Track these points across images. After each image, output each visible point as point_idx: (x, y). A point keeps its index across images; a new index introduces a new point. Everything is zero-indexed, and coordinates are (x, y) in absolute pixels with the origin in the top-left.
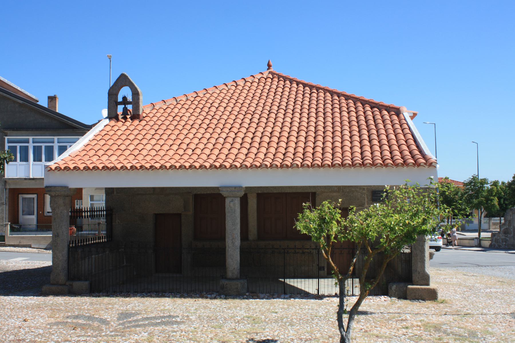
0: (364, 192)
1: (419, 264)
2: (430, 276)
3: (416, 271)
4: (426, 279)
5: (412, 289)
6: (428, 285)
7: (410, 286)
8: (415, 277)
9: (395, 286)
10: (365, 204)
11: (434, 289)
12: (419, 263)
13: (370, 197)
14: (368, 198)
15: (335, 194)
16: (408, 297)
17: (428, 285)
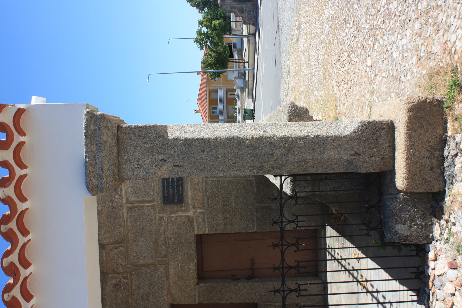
0: (166, 219)
1: (330, 154)
2: (365, 118)
3: (350, 162)
4: (378, 133)
5: (411, 174)
6: (390, 127)
7: (400, 182)
8: (369, 165)
9: (399, 227)
10: (188, 217)
11: (410, 110)
12: (327, 154)
13: (176, 207)
14: (178, 211)
15: (172, 271)
16: (436, 190)
17: (390, 127)
